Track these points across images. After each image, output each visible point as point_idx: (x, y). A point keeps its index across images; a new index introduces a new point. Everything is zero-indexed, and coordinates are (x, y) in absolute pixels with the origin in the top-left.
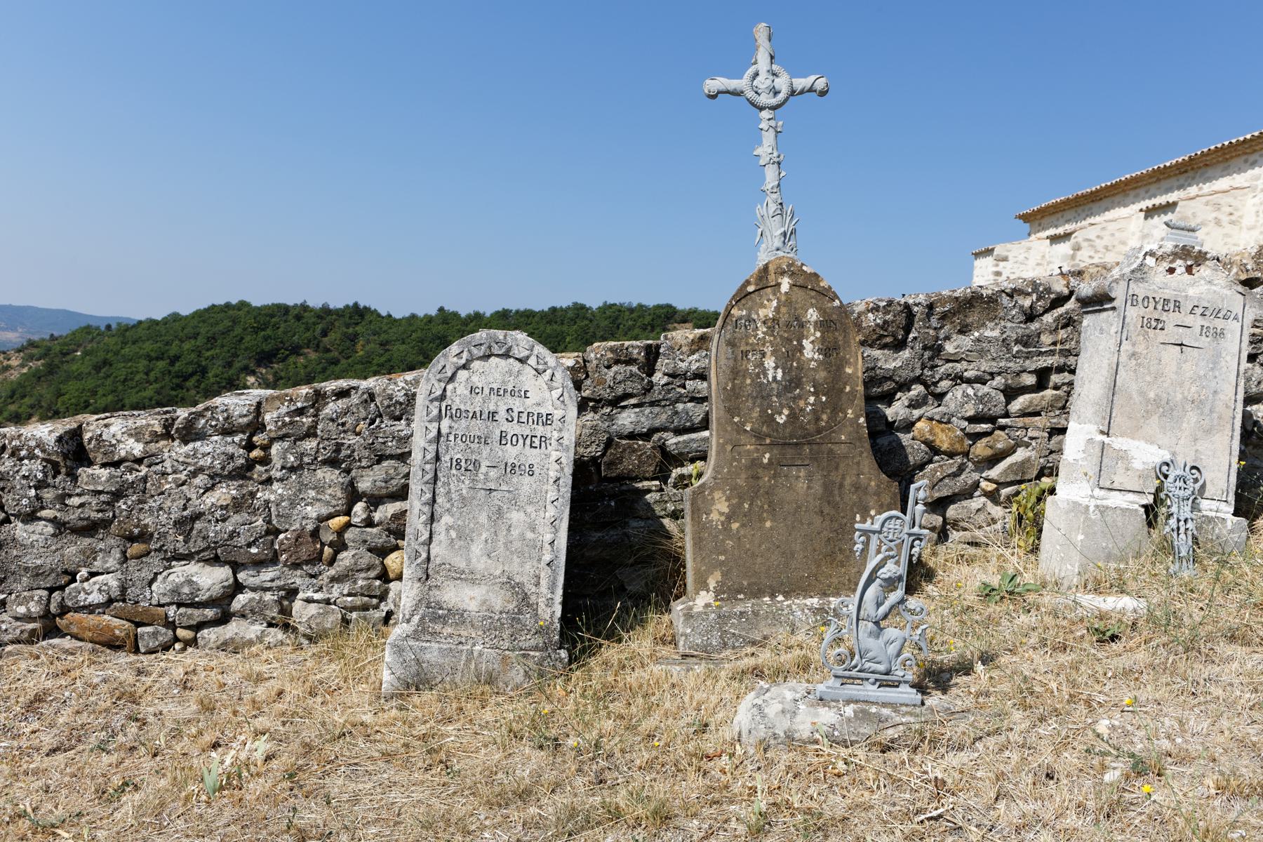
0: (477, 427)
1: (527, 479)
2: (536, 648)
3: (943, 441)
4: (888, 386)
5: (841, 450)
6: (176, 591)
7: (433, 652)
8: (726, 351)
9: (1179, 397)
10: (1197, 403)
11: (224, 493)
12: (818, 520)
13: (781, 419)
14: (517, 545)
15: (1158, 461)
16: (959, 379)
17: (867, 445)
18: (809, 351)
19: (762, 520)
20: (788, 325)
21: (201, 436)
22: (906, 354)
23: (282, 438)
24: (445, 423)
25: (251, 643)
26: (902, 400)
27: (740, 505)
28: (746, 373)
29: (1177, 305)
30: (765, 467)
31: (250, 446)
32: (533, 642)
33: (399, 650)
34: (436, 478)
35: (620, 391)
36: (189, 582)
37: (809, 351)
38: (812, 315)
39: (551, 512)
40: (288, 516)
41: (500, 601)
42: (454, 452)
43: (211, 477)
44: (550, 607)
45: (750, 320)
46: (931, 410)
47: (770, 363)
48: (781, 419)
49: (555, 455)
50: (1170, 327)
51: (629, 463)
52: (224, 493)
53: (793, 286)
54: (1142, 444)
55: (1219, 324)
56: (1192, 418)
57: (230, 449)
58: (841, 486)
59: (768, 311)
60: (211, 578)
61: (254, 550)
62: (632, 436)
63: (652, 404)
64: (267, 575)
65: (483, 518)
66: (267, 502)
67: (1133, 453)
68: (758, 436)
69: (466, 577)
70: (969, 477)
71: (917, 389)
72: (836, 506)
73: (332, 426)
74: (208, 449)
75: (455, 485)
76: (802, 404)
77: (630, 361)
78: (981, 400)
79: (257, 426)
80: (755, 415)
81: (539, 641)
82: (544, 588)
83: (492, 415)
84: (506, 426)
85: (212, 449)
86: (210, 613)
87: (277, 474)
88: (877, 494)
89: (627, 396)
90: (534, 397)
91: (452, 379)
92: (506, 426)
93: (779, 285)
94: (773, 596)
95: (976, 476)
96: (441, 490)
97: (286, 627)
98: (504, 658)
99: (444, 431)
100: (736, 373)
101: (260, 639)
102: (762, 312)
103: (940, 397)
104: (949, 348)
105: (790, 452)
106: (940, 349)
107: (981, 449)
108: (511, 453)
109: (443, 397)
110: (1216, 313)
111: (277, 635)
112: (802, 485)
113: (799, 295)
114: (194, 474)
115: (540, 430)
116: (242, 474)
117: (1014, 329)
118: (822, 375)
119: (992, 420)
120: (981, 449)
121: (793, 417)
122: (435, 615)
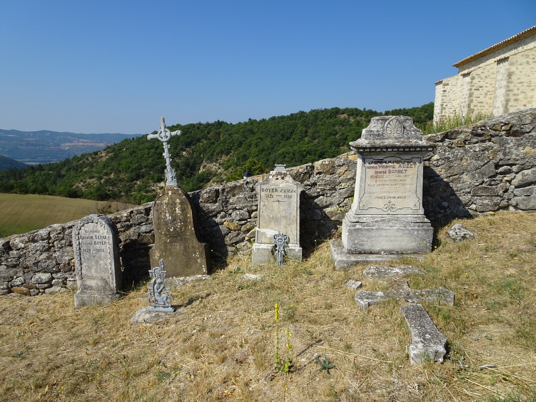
0: (89, 241)
1: (103, 253)
2: (110, 295)
3: (232, 227)
4: (214, 213)
5: (188, 237)
6: (37, 280)
7: (85, 296)
8: (156, 213)
9: (279, 216)
10: (285, 217)
11: (45, 255)
12: (183, 257)
13: (172, 230)
14: (103, 269)
15: (274, 234)
16: (235, 209)
17: (195, 235)
18: (178, 211)
19: (168, 257)
20: (172, 204)
21: (37, 241)
22: (217, 204)
23: (56, 240)
24: (81, 240)
25: (57, 292)
26: (219, 216)
27: (162, 254)
28: (161, 218)
29: (276, 190)
30: (168, 243)
31: (49, 243)
32: (109, 293)
33: (77, 297)
34: (80, 254)
35: (140, 221)
36: (40, 278)
37: (178, 211)
38: (178, 201)
39: (109, 261)
40: (61, 260)
41: (100, 283)
42: (84, 247)
43: (41, 251)
44: (113, 284)
45: (162, 204)
46: (228, 218)
47: (167, 215)
48: (172, 230)
49: (108, 246)
50: (275, 197)
51: (145, 240)
52: (45, 255)
53: (172, 193)
54: (270, 230)
55: (290, 194)
56: (284, 221)
57: (44, 244)
58: (189, 247)
59: (166, 201)
60: (45, 277)
61: (54, 269)
62: (146, 232)
63: (149, 224)
64: (59, 275)
65: (93, 263)
66: (55, 257)
67: (267, 233)
68: (166, 235)
69: (92, 278)
70: (240, 237)
71: (223, 213)
72: (187, 252)
73: (68, 237)
74: (38, 245)
75: (85, 255)
76: (177, 225)
77: (141, 213)
78: (241, 215)
79: (49, 238)
80: (165, 229)
81: (111, 293)
82: (111, 280)
83: (92, 237)
84: (95, 240)
85: (39, 245)
86: (46, 285)
87: (57, 250)
88: (198, 248)
89: (142, 222)
90: (101, 232)
91: (80, 229)
92: (95, 240)
93: (168, 193)
94: (172, 277)
95: (244, 235)
96: (82, 257)
97: (66, 287)
98: (103, 298)
99: (81, 242)
100: (159, 218)
101: (59, 291)
102: (164, 201)
103: (230, 214)
104: (231, 201)
105: (174, 239)
106: (228, 201)
107: (243, 228)
108: (98, 246)
109: (79, 234)
110: (289, 191)
111: (63, 289)
112: (178, 247)
113: (174, 195)
114: (37, 251)
115: (104, 240)
116: (48, 250)
117: (248, 194)
118: (181, 217)
119: (246, 220)
120: (243, 228)
121: (175, 229)
122: (85, 288)
